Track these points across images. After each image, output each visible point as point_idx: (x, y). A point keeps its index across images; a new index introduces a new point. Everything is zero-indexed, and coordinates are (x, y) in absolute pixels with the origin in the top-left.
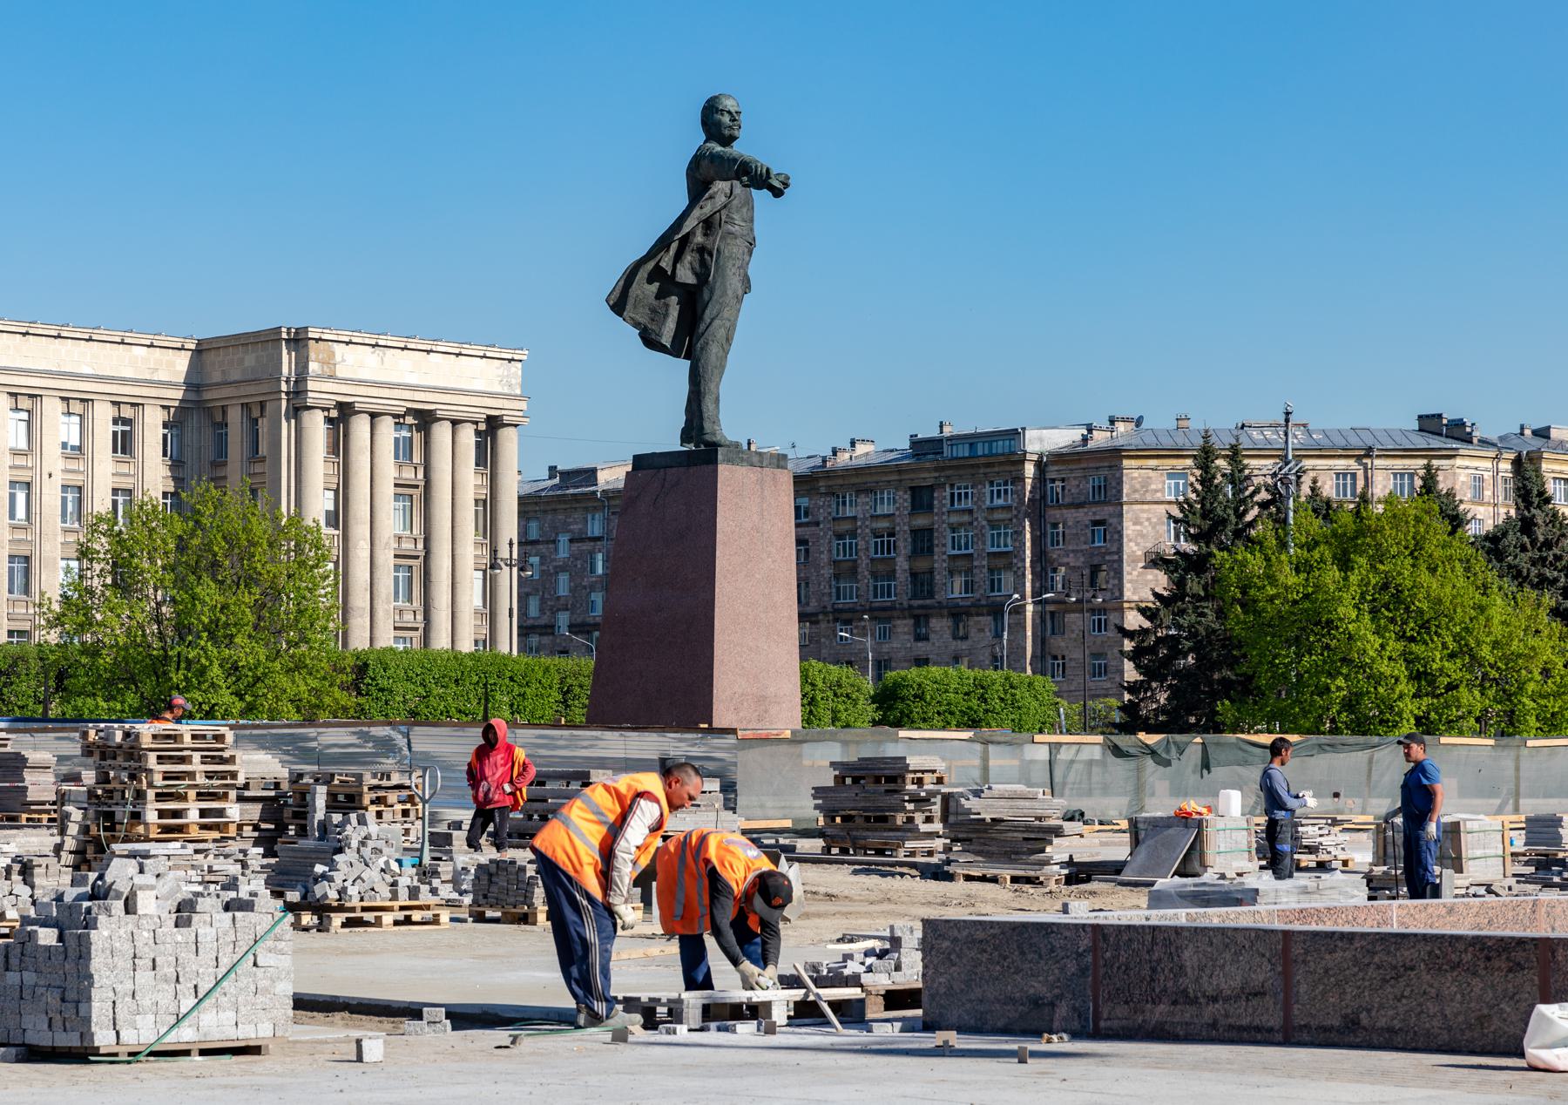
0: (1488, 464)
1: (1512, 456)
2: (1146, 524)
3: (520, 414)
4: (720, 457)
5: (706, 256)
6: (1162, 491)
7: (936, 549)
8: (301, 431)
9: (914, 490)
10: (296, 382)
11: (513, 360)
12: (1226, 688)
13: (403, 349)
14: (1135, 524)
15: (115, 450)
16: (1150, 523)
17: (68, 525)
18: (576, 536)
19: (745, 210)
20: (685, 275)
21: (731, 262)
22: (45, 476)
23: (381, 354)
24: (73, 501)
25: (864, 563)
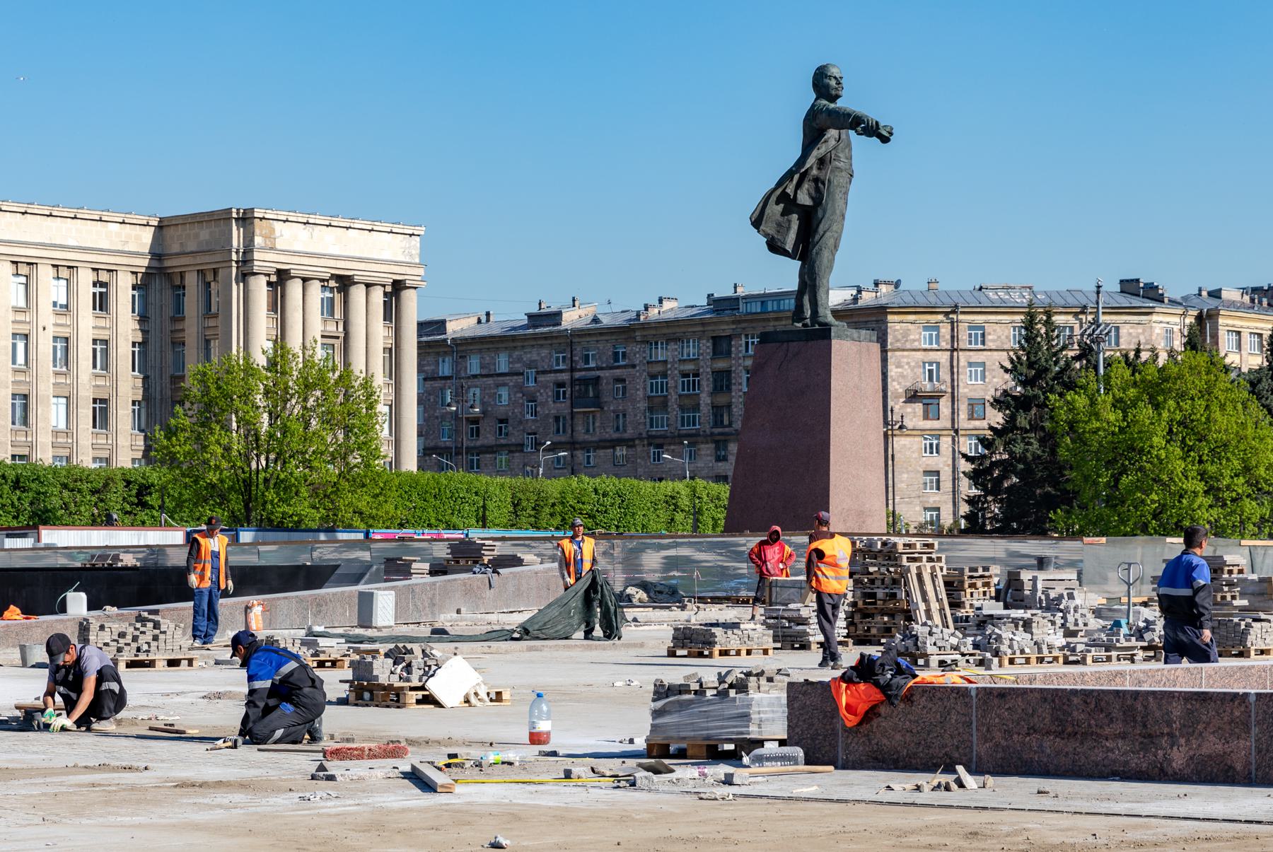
0: (1176, 319)
1: (1195, 313)
2: (907, 367)
3: (419, 278)
4: (833, 334)
5: (820, 185)
6: (919, 340)
7: (734, 387)
8: (248, 293)
9: (716, 340)
10: (244, 253)
11: (413, 235)
12: (1051, 503)
13: (327, 226)
14: (897, 367)
15: (94, 308)
16: (910, 366)
17: (58, 369)
18: (429, 376)
19: (847, 150)
20: (804, 198)
21: (839, 189)
22: (40, 329)
23: (311, 230)
24: (61, 349)
25: (673, 398)
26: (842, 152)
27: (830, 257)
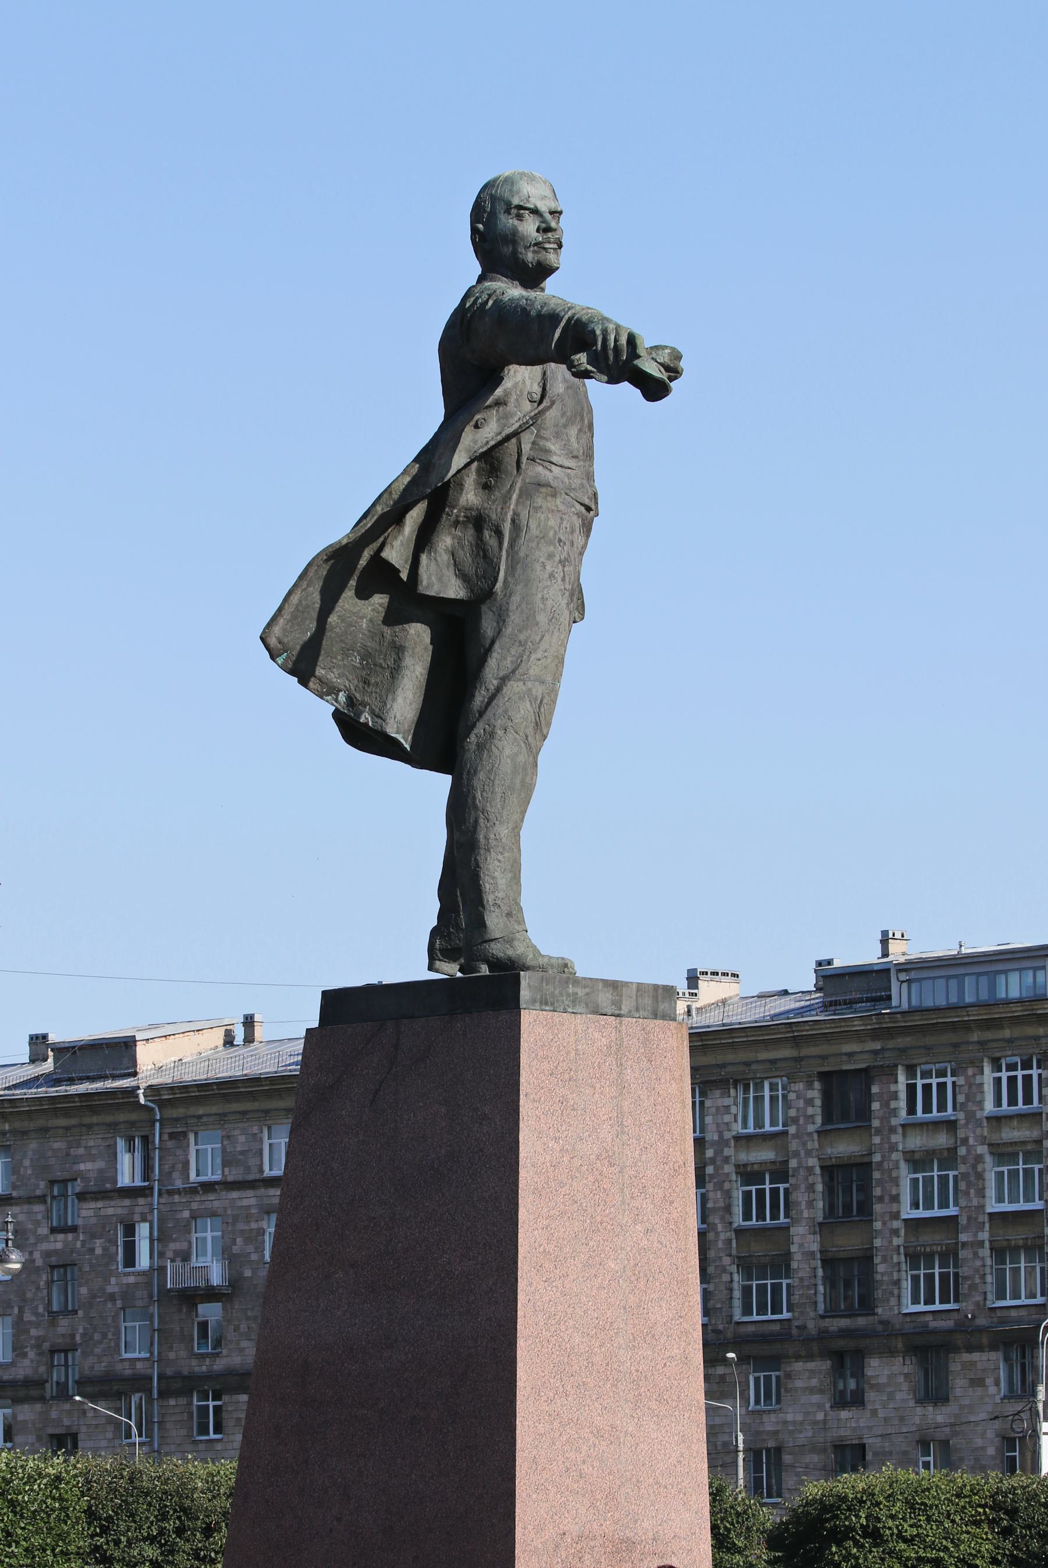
4: (525, 994)
7: (877, 1208)
18: (92, 1186)
19: (573, 431)
26: (557, 435)
27: (521, 759)
